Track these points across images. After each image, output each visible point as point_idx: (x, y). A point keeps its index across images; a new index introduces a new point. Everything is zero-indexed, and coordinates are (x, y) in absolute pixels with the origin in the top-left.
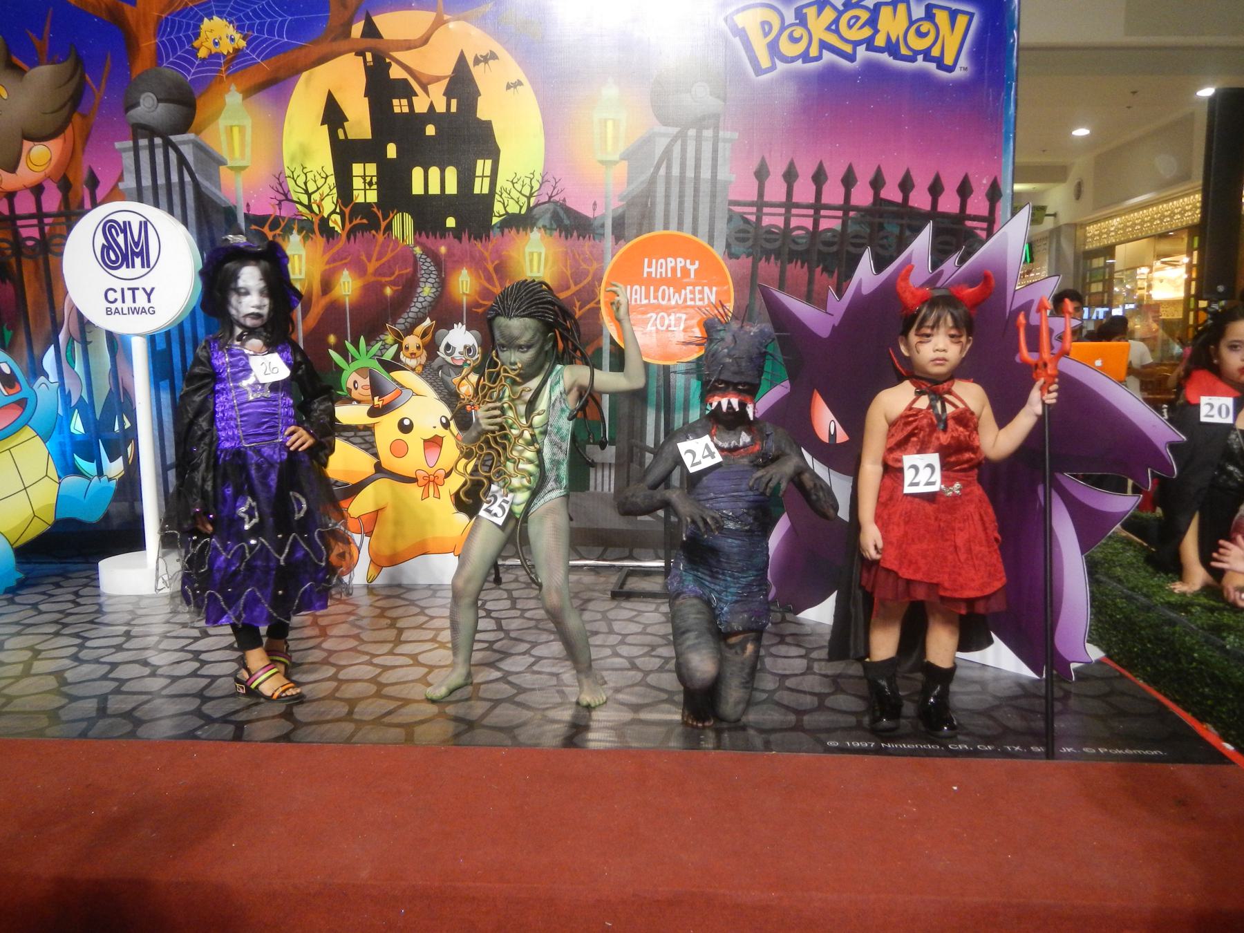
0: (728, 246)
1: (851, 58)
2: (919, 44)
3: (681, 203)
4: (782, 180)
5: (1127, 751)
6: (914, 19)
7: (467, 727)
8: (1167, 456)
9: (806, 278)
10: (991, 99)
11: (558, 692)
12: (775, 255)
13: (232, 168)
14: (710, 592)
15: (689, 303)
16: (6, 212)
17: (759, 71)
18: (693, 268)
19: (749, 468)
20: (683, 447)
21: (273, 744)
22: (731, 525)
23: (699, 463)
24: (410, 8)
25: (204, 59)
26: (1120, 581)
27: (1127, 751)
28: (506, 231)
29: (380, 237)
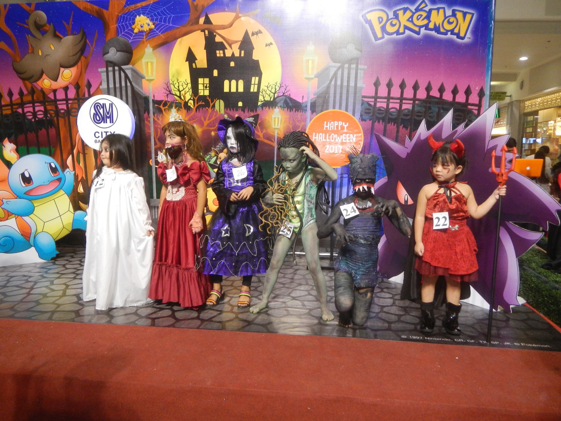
0: (361, 115)
1: (418, 33)
2: (448, 27)
3: (341, 97)
4: (386, 86)
5: (534, 345)
6: (447, 16)
7: (247, 324)
8: (556, 216)
9: (396, 130)
11: (285, 310)
12: (382, 120)
13: (148, 80)
14: (352, 270)
15: (344, 141)
16: (53, 98)
17: (377, 39)
18: (346, 126)
19: (371, 217)
20: (342, 208)
21: (167, 328)
22: (362, 241)
23: (349, 215)
24: (224, 11)
25: (137, 33)
26: (534, 269)
27: (534, 345)
28: (264, 108)
29: (210, 110)
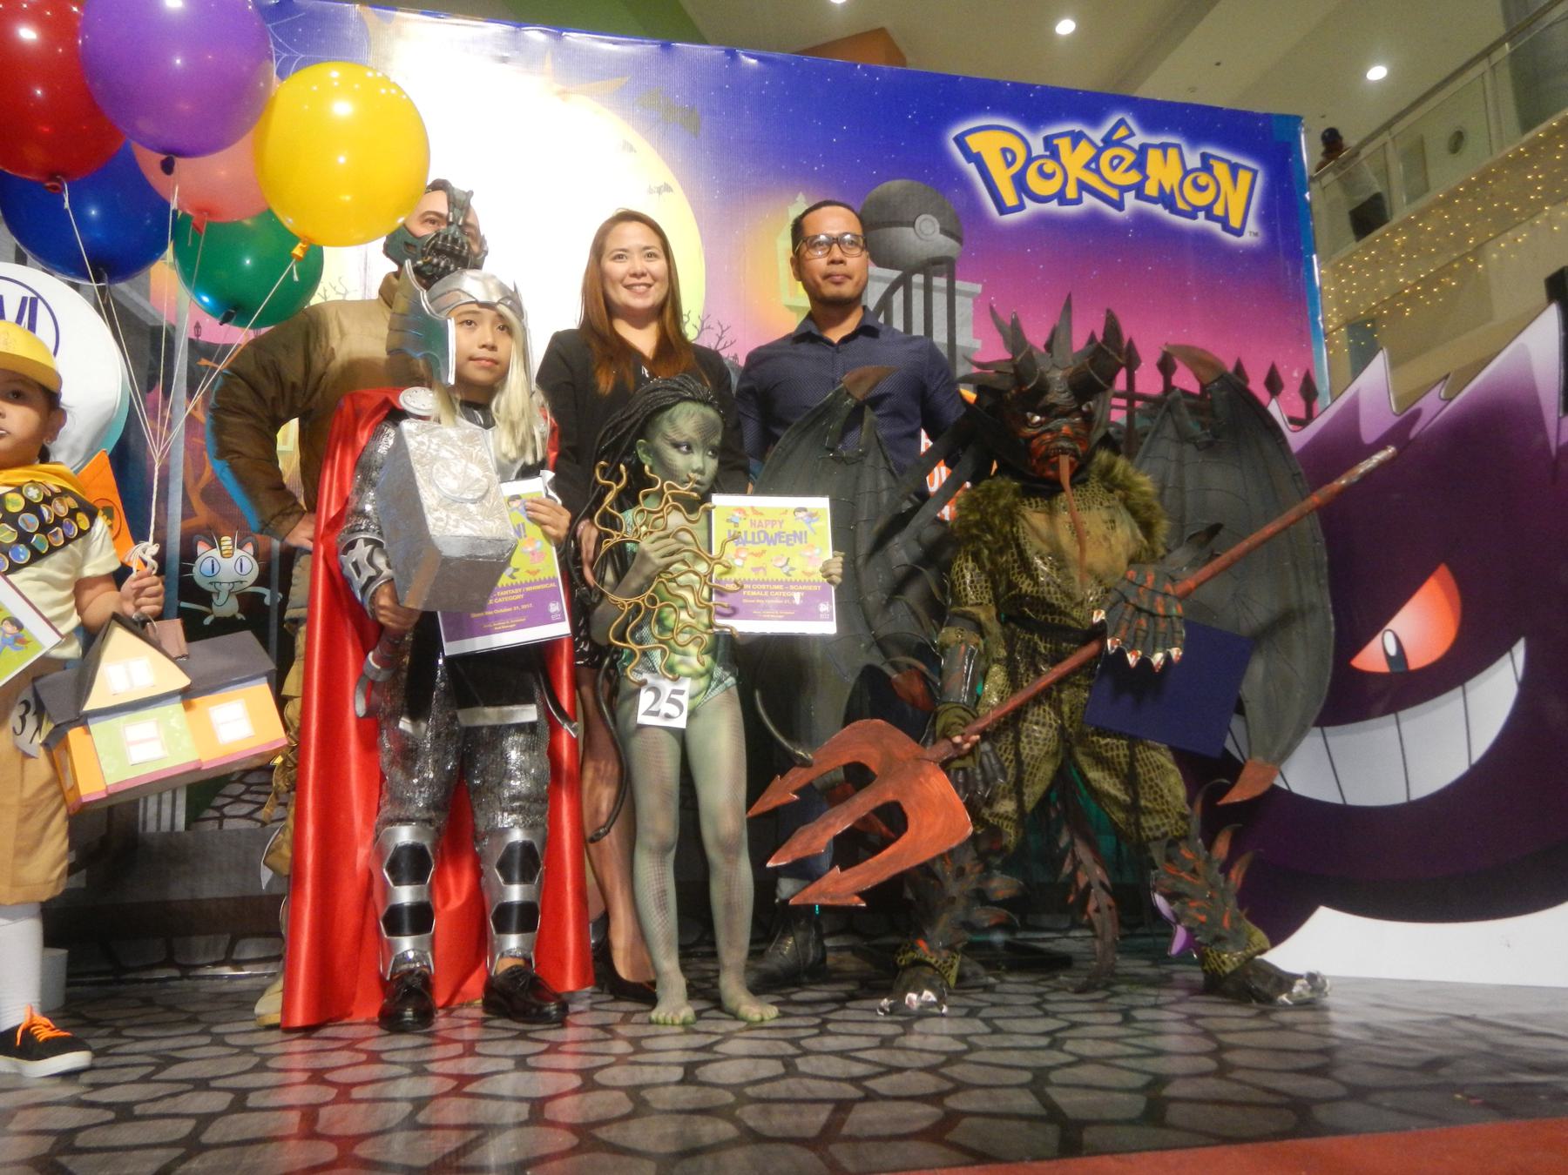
1: (1119, 205)
6: (1189, 167)
10: (1289, 273)
17: (1003, 209)
